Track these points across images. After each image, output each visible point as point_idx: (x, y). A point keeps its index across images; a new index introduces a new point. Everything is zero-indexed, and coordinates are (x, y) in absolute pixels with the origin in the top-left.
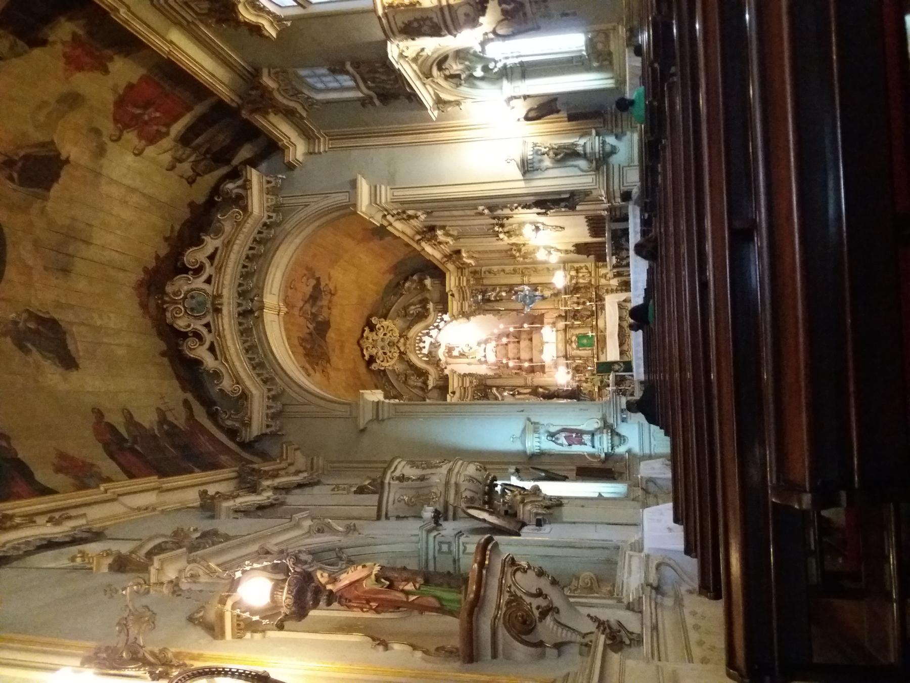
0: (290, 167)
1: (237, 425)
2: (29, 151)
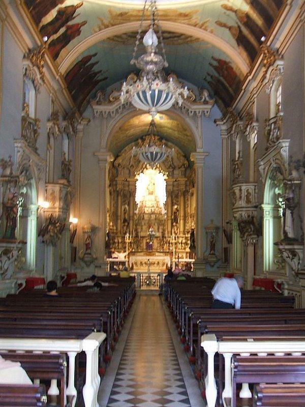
0: (215, 122)
1: (98, 99)
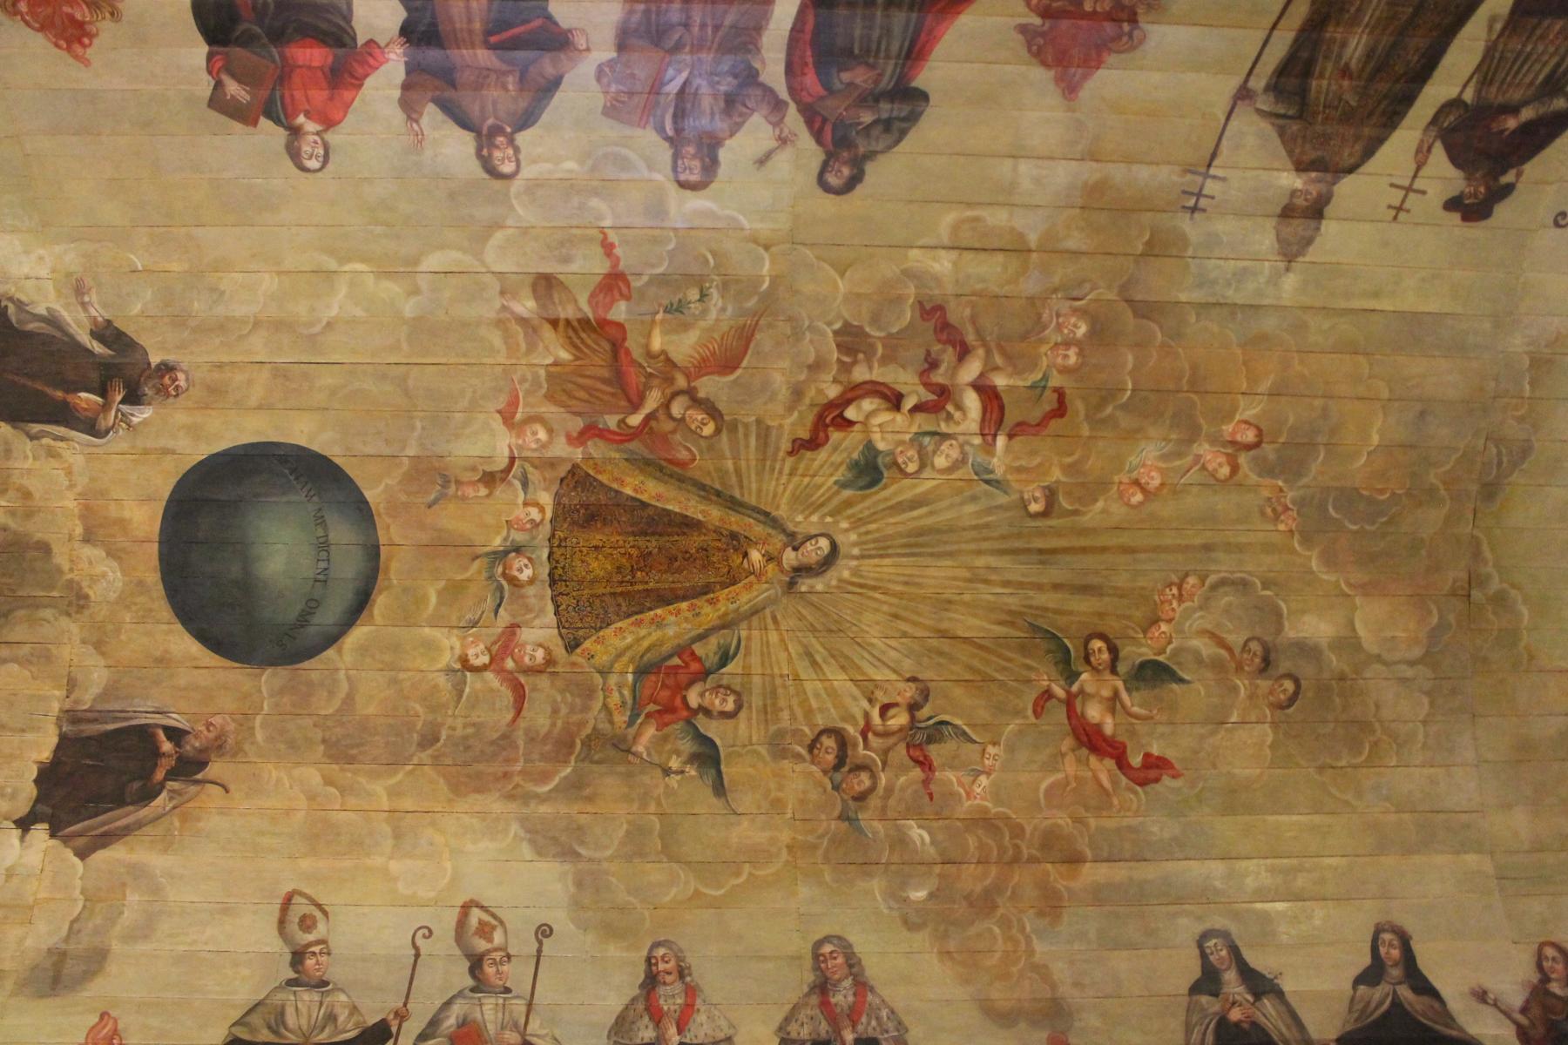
2: (145, 812)
